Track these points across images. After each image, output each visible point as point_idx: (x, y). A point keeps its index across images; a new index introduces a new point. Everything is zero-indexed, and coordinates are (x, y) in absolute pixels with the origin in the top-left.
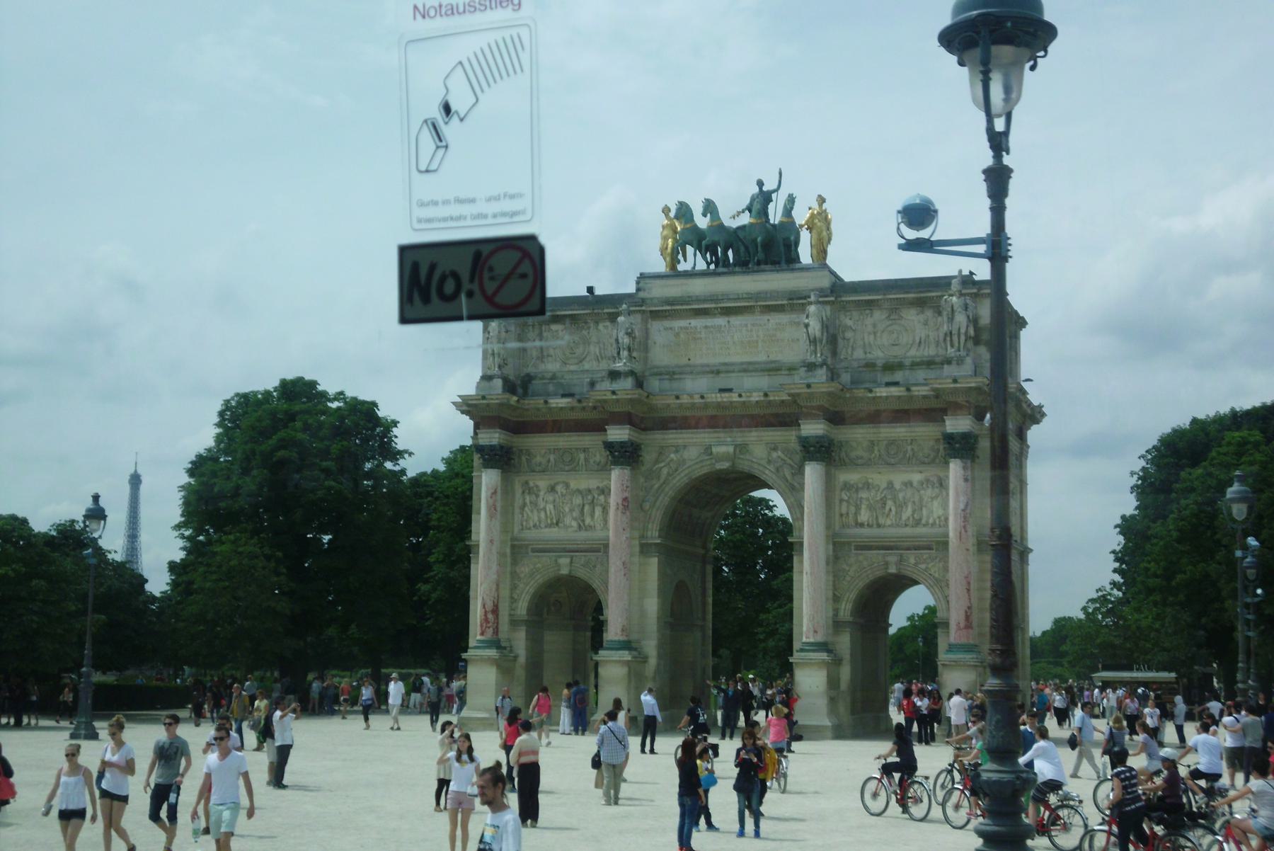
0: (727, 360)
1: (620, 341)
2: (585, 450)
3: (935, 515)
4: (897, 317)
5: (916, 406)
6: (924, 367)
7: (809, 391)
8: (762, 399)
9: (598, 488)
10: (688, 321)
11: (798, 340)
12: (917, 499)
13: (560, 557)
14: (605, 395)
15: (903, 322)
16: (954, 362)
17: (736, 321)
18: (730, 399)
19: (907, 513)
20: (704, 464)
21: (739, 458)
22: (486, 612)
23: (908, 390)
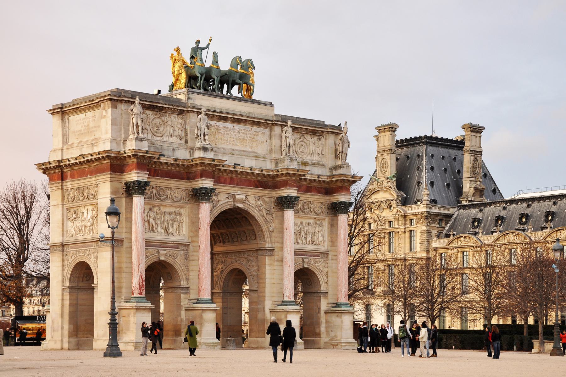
0: (233, 148)
1: (203, 129)
2: (171, 189)
3: (320, 240)
4: (304, 138)
5: (318, 185)
6: (317, 166)
7: (297, 173)
8: (260, 172)
9: (175, 211)
10: (215, 122)
11: (264, 142)
12: (313, 232)
13: (161, 250)
14: (209, 161)
15: (305, 141)
16: (345, 167)
17: (238, 126)
18: (246, 171)
19: (309, 238)
20: (228, 204)
21: (244, 203)
22: (143, 281)
23: (318, 177)
